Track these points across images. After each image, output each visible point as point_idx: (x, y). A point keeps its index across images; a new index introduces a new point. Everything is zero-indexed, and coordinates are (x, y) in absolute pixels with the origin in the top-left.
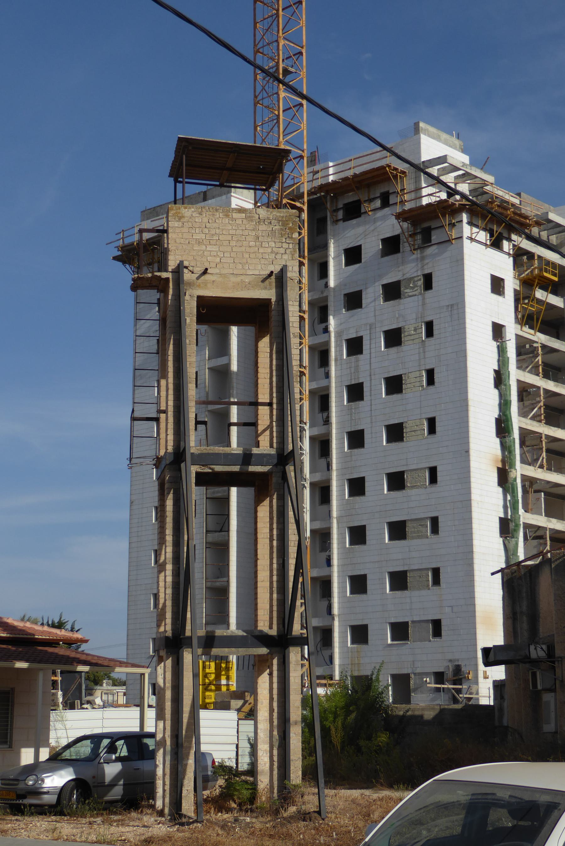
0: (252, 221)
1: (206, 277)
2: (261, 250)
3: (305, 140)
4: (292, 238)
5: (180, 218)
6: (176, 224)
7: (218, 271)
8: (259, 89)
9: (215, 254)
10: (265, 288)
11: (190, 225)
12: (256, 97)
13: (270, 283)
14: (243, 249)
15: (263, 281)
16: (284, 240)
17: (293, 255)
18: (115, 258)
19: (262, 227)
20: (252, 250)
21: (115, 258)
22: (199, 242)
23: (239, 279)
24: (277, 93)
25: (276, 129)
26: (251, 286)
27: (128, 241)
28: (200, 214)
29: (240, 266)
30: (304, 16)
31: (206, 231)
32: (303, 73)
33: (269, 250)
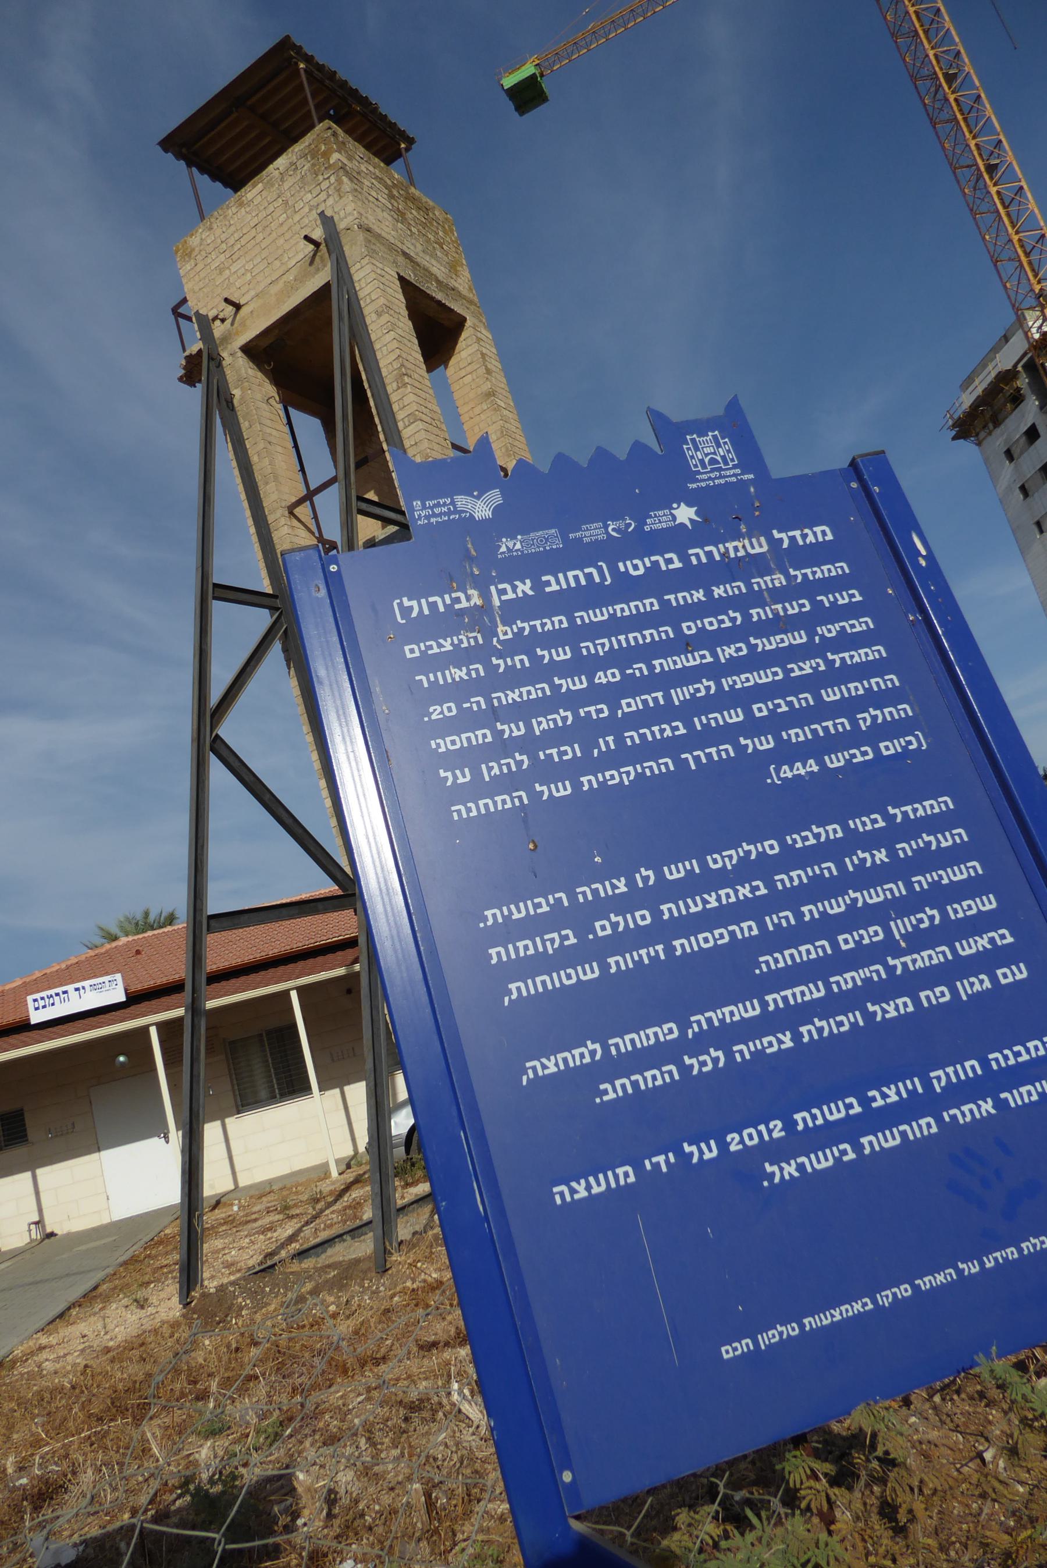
0: (272, 185)
1: (243, 311)
2: (297, 218)
3: (1039, 217)
4: (330, 166)
5: (189, 255)
6: (188, 267)
7: (252, 293)
8: (970, 200)
9: (242, 271)
10: (318, 270)
11: (203, 253)
12: (972, 210)
13: (322, 260)
14: (274, 235)
15: (311, 263)
16: (321, 178)
17: (338, 190)
18: (954, 438)
19: (289, 182)
20: (285, 228)
21: (954, 438)
22: (221, 270)
23: (281, 284)
24: (989, 192)
25: (1001, 227)
26: (300, 279)
27: (956, 417)
28: (211, 229)
29: (277, 263)
30: (988, 106)
31: (224, 246)
32: (1010, 157)
33: (307, 209)
